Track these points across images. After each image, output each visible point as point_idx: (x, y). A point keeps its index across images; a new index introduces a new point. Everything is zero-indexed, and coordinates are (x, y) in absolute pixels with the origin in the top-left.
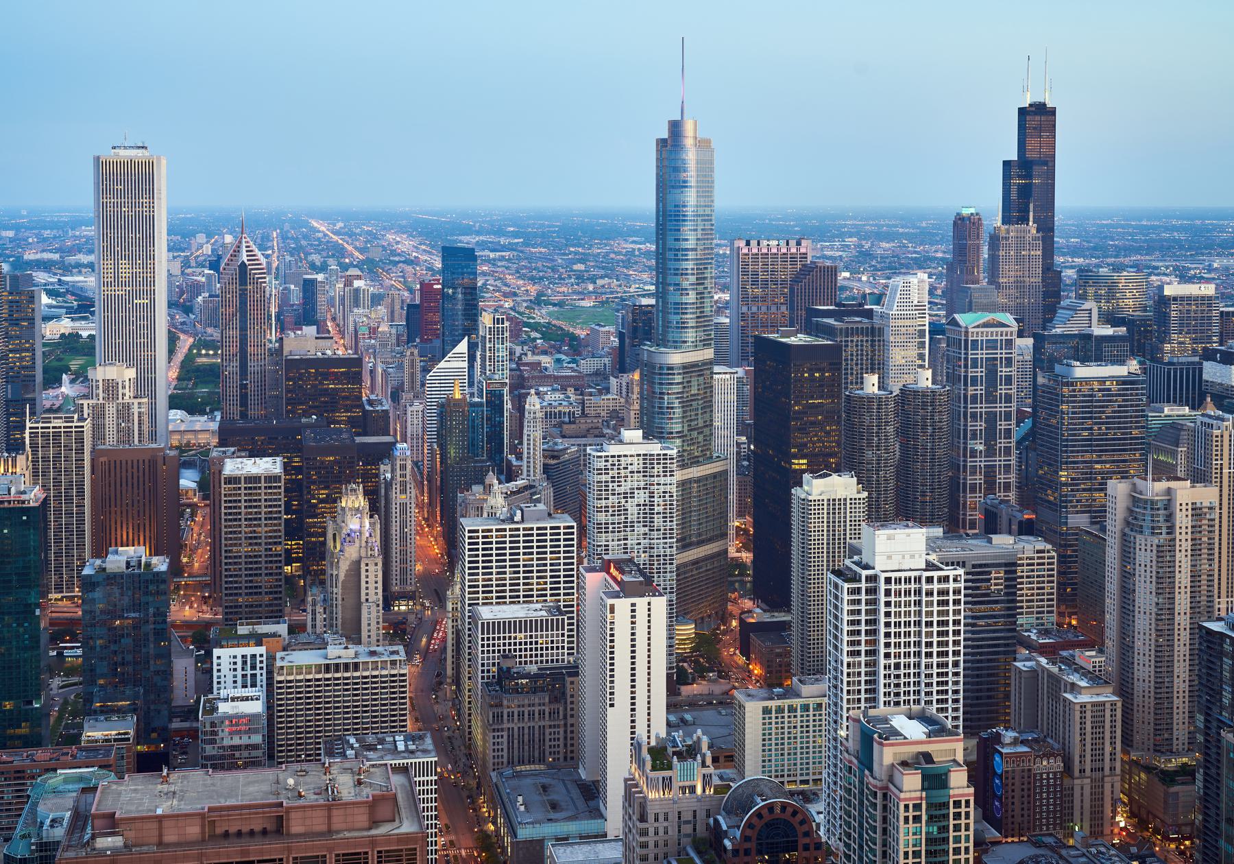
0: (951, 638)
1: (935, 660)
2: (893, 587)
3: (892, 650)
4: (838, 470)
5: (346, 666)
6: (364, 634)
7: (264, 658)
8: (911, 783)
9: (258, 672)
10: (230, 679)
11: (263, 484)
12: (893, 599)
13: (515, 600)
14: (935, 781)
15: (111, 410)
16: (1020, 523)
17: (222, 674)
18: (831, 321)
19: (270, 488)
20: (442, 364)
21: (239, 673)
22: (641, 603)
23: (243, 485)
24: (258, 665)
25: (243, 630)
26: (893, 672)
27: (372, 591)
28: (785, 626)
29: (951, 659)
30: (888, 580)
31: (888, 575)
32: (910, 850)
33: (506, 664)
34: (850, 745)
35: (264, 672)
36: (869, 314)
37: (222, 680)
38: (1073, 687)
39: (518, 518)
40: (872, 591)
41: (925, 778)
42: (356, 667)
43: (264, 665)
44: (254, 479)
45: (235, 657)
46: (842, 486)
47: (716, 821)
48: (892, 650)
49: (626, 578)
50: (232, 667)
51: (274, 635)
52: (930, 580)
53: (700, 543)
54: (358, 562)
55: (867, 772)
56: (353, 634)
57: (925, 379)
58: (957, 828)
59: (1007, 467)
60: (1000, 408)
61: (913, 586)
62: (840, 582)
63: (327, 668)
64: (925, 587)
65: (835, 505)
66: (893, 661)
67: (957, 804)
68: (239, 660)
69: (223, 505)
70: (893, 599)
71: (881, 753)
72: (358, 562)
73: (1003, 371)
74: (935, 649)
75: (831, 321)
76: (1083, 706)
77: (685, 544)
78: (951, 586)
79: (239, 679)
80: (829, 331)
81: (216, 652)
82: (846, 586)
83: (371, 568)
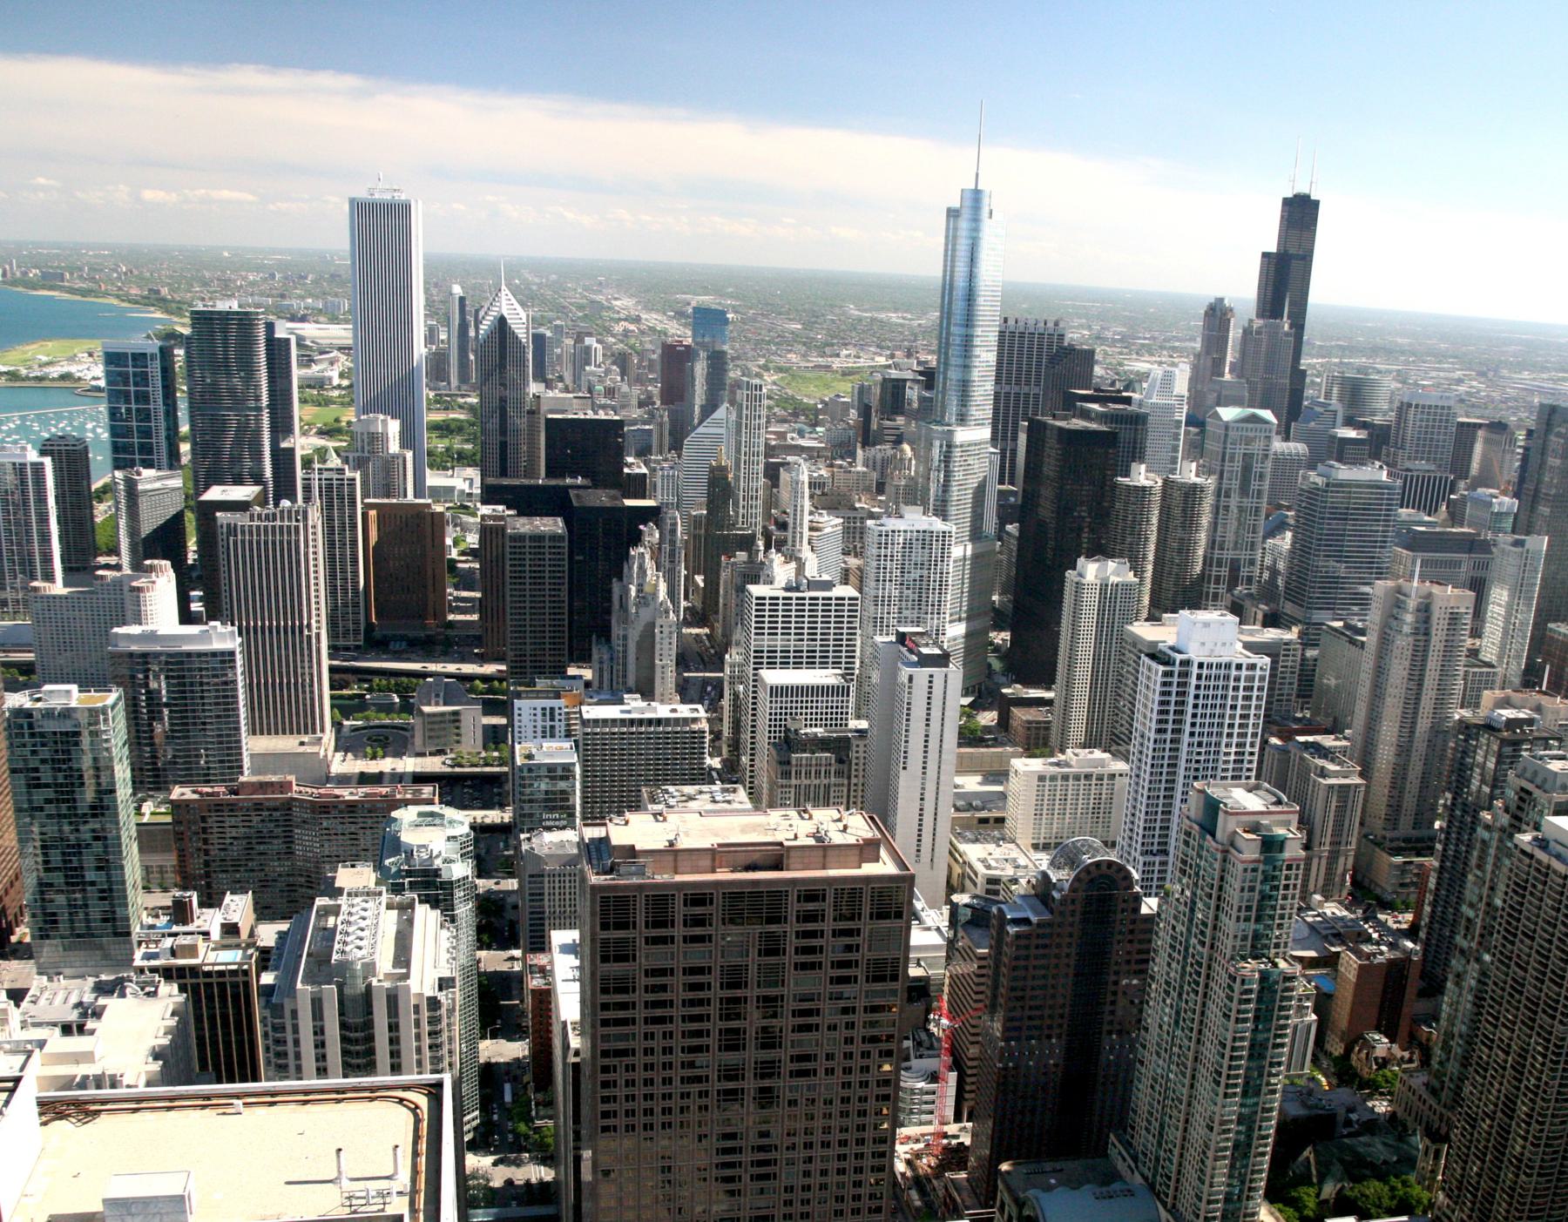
3: (1197, 730)
5: (650, 722)
6: (658, 691)
8: (1249, 849)
11: (547, 544)
16: (1265, 616)
20: (701, 430)
21: (540, 724)
30: (1201, 666)
31: (1202, 659)
32: (1244, 905)
36: (1128, 401)
38: (1323, 773)
42: (659, 722)
44: (538, 538)
46: (1114, 571)
48: (1197, 730)
55: (1209, 837)
56: (647, 693)
58: (1286, 887)
61: (1223, 672)
62: (1154, 665)
64: (1234, 673)
66: (1196, 739)
68: (539, 712)
71: (1225, 822)
72: (653, 625)
73: (1257, 468)
75: (1095, 406)
76: (1331, 787)
78: (1258, 673)
79: (539, 729)
82: (1162, 668)
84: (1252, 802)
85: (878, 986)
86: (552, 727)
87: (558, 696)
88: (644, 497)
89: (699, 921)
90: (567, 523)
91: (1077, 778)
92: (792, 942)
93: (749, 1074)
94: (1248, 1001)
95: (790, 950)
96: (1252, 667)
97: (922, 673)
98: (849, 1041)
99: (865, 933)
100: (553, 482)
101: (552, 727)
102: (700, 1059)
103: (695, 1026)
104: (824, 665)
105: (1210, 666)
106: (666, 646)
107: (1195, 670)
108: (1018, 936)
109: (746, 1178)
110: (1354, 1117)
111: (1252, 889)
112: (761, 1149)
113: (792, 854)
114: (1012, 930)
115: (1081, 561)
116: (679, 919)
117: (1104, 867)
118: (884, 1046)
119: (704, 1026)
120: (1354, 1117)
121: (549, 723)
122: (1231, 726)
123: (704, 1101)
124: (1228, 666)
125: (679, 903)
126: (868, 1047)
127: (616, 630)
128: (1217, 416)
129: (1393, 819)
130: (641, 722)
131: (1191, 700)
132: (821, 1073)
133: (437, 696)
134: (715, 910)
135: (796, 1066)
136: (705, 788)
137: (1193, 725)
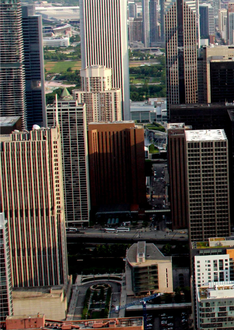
7: (228, 262)
11: (214, 147)
15: (95, 98)
17: (201, 272)
19: (219, 150)
21: (212, 272)
23: (201, 148)
24: (225, 267)
25: (213, 243)
35: (228, 271)
37: (201, 276)
43: (228, 266)
44: (209, 144)
45: (209, 261)
50: (208, 268)
68: (212, 264)
69: (188, 161)
79: (212, 276)
81: (197, 258)
86: (222, 274)
87: (224, 252)
100: (218, 106)
101: (222, 274)
121: (219, 271)
133: (141, 255)
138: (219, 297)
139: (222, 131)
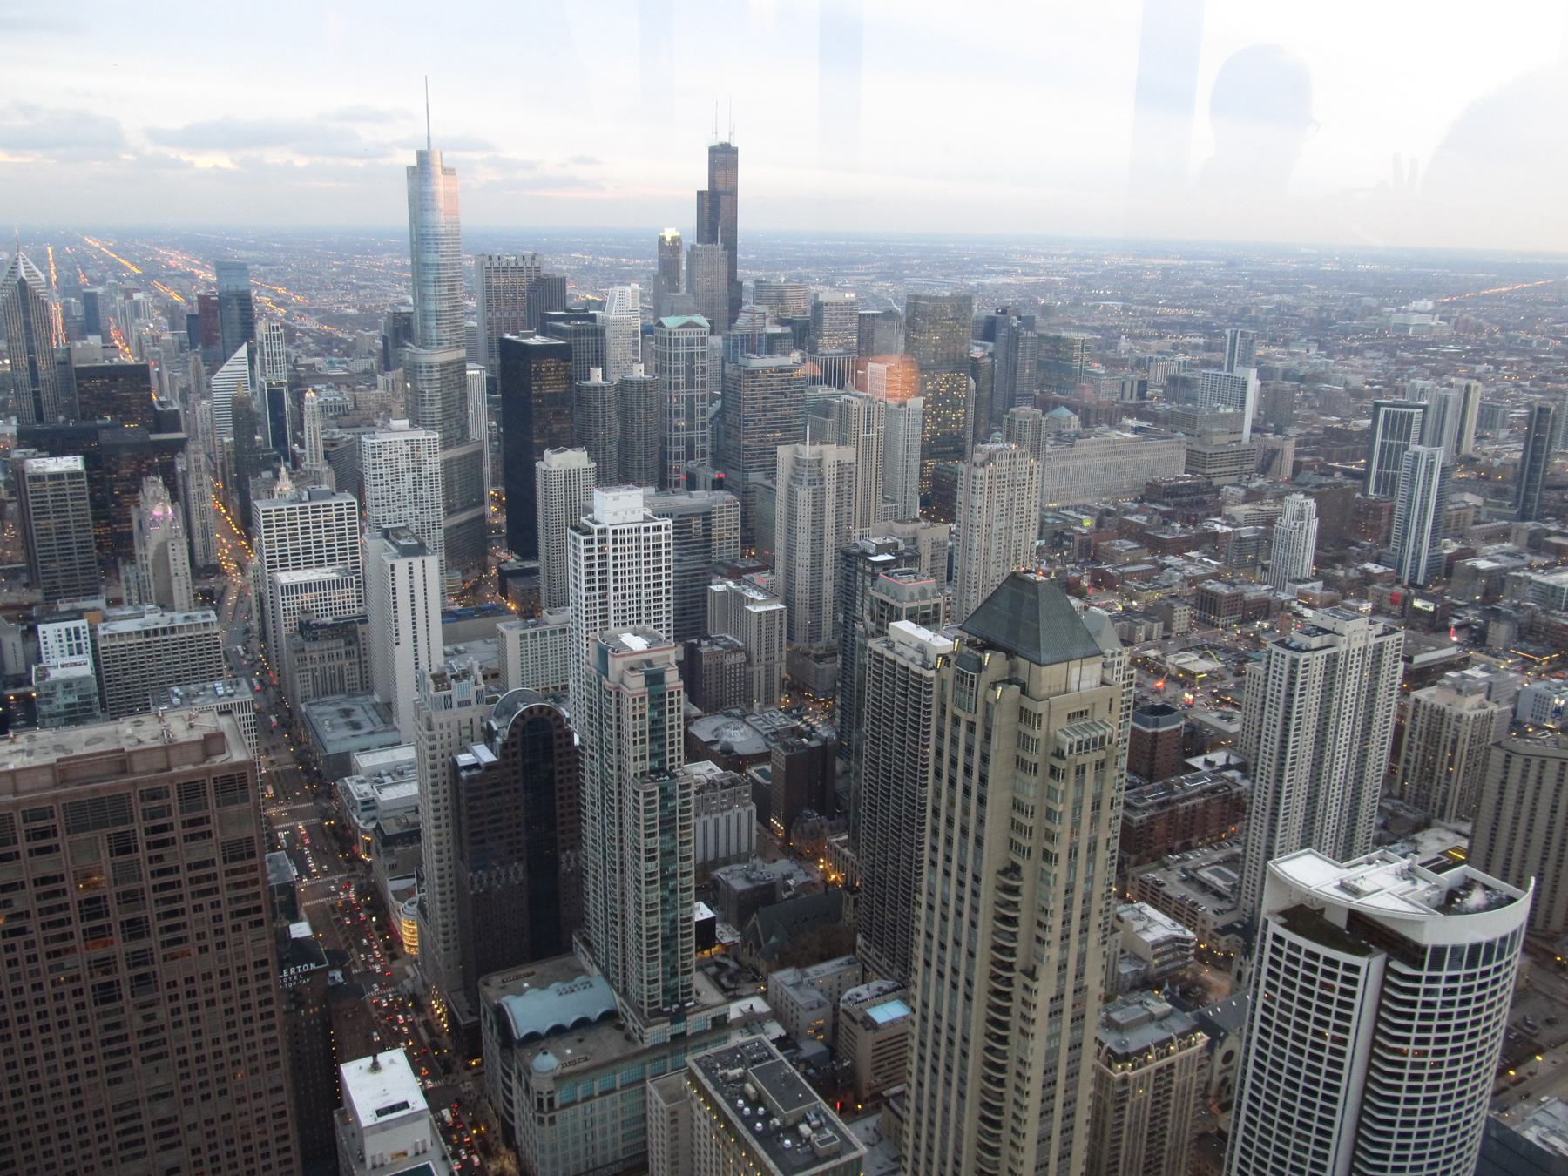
0: (664, 572)
1: (652, 589)
2: (619, 537)
3: (619, 585)
4: (571, 446)
5: (164, 631)
6: (177, 603)
8: (636, 683)
9: (82, 641)
10: (57, 649)
12: (619, 546)
13: (308, 565)
14: (655, 678)
18: (562, 324)
20: (225, 368)
21: (65, 643)
22: (417, 561)
25: (63, 606)
26: (620, 601)
27: (180, 567)
28: (535, 571)
29: (664, 587)
33: (304, 618)
34: (590, 658)
36: (593, 318)
39: (306, 497)
40: (603, 541)
41: (647, 677)
42: (173, 630)
46: (575, 459)
47: (489, 725)
48: (619, 585)
49: (403, 542)
51: (94, 609)
52: (647, 530)
53: (463, 510)
54: (165, 544)
56: (166, 604)
57: (639, 372)
59: (703, 439)
60: (698, 392)
61: (634, 535)
63: (147, 633)
64: (643, 535)
65: (572, 475)
66: (620, 593)
67: (671, 694)
70: (619, 546)
72: (165, 544)
73: (698, 362)
74: (652, 582)
75: (562, 324)
76: (760, 614)
77: (450, 511)
79: (66, 649)
80: (559, 333)
81: (41, 628)
82: (582, 538)
83: (177, 547)
84: (637, 643)
85: (237, 865)
88: (179, 430)
89: (44, 833)
90: (86, 461)
91: (553, 632)
92: (142, 839)
93: (122, 964)
94: (653, 810)
95: (142, 846)
96: (658, 528)
97: (402, 565)
98: (218, 918)
99: (214, 819)
100: (85, 424)
101: (79, 645)
102: (68, 961)
103: (58, 931)
104: (320, 563)
105: (623, 532)
106: (179, 562)
107: (610, 537)
108: (471, 779)
109: (137, 1062)
110: (791, 882)
111: (642, 716)
112: (147, 1032)
113: (135, 757)
114: (464, 774)
115: (547, 452)
116: (21, 836)
117: (536, 712)
118: (254, 917)
119: (67, 929)
120: (791, 882)
122: (647, 578)
123: (79, 999)
124: (638, 530)
125: (18, 818)
126: (236, 921)
127: (138, 551)
128: (660, 324)
129: (815, 634)
130: (155, 632)
131: (611, 562)
132: (195, 952)
134: (59, 821)
135: (167, 951)
136: (209, 686)
137: (616, 581)
138: (63, 676)
139: (79, 458)
